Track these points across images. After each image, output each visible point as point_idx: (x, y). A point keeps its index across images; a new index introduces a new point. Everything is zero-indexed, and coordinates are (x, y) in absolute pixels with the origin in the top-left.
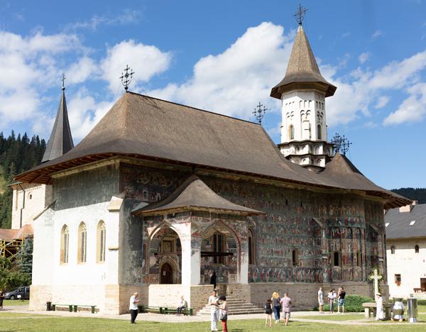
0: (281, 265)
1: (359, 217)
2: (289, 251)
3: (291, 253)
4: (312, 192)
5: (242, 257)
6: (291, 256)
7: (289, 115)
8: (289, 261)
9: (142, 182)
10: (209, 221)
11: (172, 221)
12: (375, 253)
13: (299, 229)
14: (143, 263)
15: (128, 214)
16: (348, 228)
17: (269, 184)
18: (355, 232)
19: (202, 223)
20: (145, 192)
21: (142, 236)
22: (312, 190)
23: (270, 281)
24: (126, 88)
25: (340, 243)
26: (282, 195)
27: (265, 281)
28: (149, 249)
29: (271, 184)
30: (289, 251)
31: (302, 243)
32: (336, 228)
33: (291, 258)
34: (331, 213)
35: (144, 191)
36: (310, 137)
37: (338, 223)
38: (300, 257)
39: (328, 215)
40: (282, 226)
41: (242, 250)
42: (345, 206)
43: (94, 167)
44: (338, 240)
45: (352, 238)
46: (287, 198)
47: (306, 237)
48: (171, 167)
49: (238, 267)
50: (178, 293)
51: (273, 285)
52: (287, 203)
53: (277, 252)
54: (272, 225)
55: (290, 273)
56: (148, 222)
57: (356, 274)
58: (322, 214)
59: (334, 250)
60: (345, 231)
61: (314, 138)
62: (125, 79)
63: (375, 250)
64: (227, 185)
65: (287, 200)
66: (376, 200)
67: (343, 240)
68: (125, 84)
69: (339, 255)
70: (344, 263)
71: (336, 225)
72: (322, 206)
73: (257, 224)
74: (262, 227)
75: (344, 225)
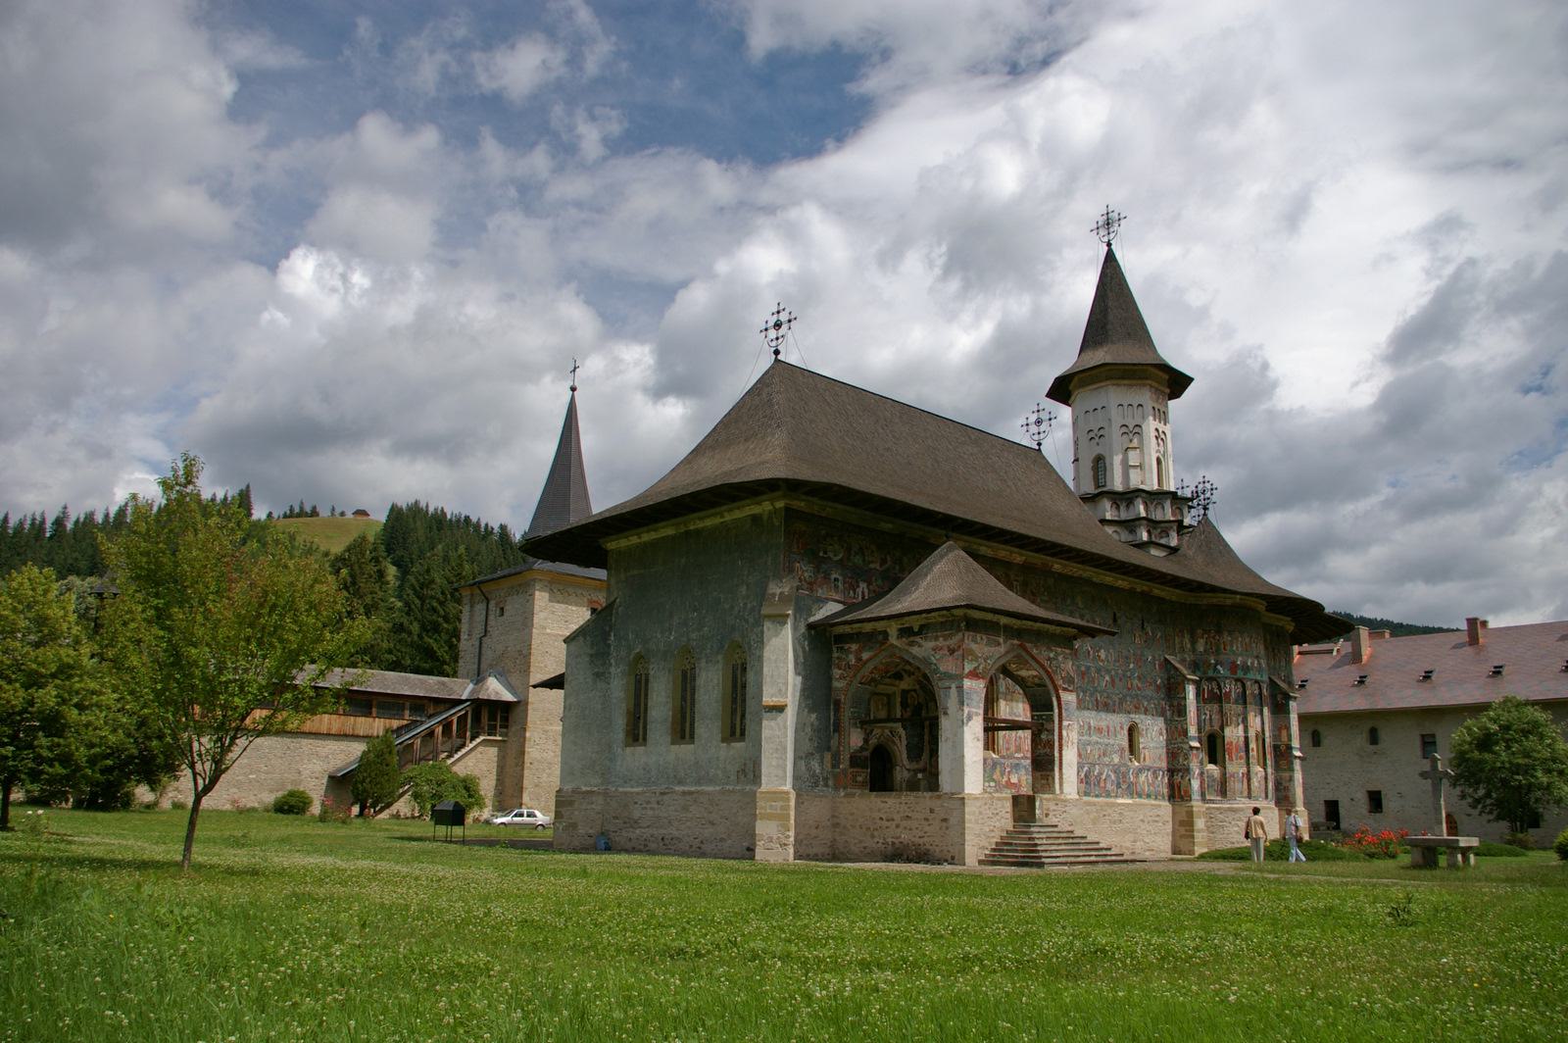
1: (1257, 657)
2: (1122, 728)
3: (1126, 732)
4: (1162, 599)
5: (1064, 733)
6: (1126, 738)
7: (1092, 435)
9: (831, 555)
10: (999, 644)
11: (911, 644)
12: (1284, 739)
13: (1139, 678)
14: (834, 743)
15: (803, 629)
16: (1237, 680)
17: (1080, 578)
18: (1252, 690)
19: (986, 649)
20: (836, 580)
21: (830, 679)
22: (1162, 594)
24: (777, 352)
25: (1221, 711)
28: (847, 713)
29: (1086, 575)
30: (1122, 728)
32: (1210, 679)
33: (1125, 743)
34: (1201, 648)
35: (833, 576)
36: (1142, 483)
37: (1215, 669)
38: (1142, 742)
39: (1194, 650)
40: (1108, 672)
41: (1064, 714)
42: (1230, 633)
43: (718, 520)
44: (1216, 706)
45: (1245, 703)
47: (1151, 698)
48: (890, 526)
49: (1057, 754)
50: (932, 811)
53: (1099, 730)
54: (1088, 668)
55: (1124, 777)
56: (846, 647)
57: (1255, 783)
58: (1182, 650)
59: (1208, 728)
60: (1231, 688)
61: (1152, 485)
62: (772, 334)
63: (1284, 733)
65: (1115, 615)
67: (1226, 706)
68: (774, 344)
69: (1219, 741)
70: (1231, 759)
71: (1210, 673)
72: (1181, 631)
75: (1228, 674)
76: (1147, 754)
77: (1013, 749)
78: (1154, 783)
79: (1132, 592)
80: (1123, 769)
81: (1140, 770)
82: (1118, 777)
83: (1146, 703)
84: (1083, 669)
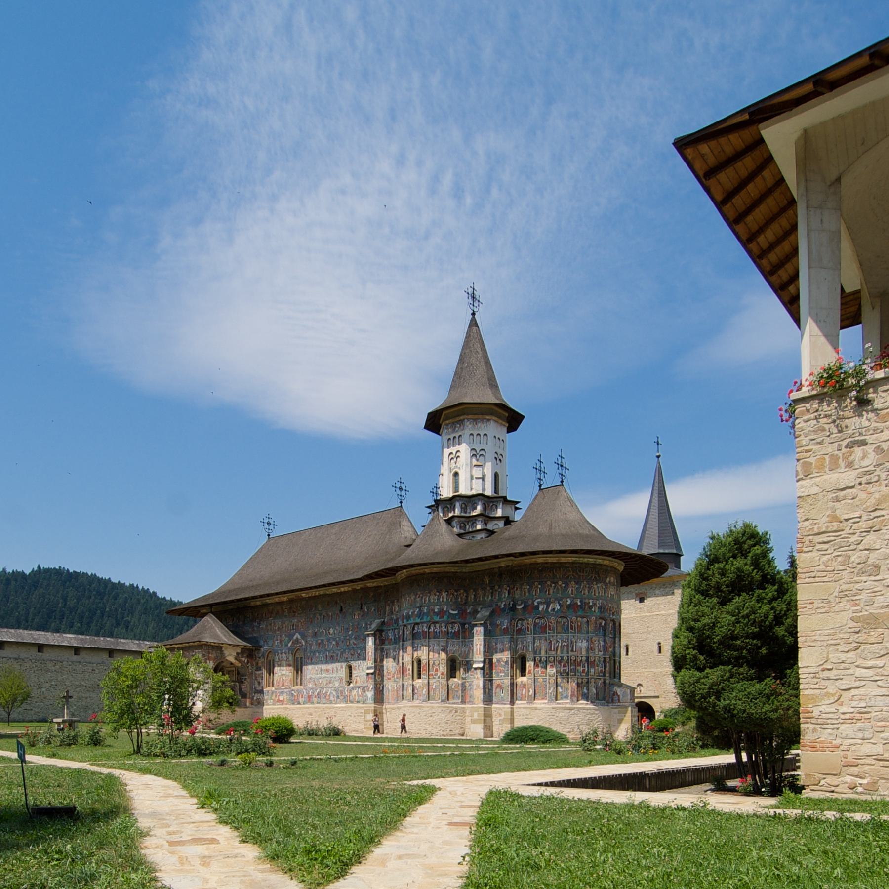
0: (331, 685)
8: (342, 679)
13: (355, 638)
22: (375, 584)
23: (317, 703)
26: (336, 603)
27: (312, 703)
29: (321, 593)
31: (359, 655)
40: (334, 639)
46: (342, 604)
51: (319, 708)
52: (341, 610)
54: (322, 640)
55: (342, 693)
64: (278, 608)
65: (341, 607)
66: (503, 564)
73: (306, 642)
74: (311, 645)
76: (358, 679)
77: (281, 685)
78: (362, 695)
79: (355, 591)
80: (340, 689)
81: (353, 689)
82: (337, 693)
83: (359, 652)
84: (319, 641)
